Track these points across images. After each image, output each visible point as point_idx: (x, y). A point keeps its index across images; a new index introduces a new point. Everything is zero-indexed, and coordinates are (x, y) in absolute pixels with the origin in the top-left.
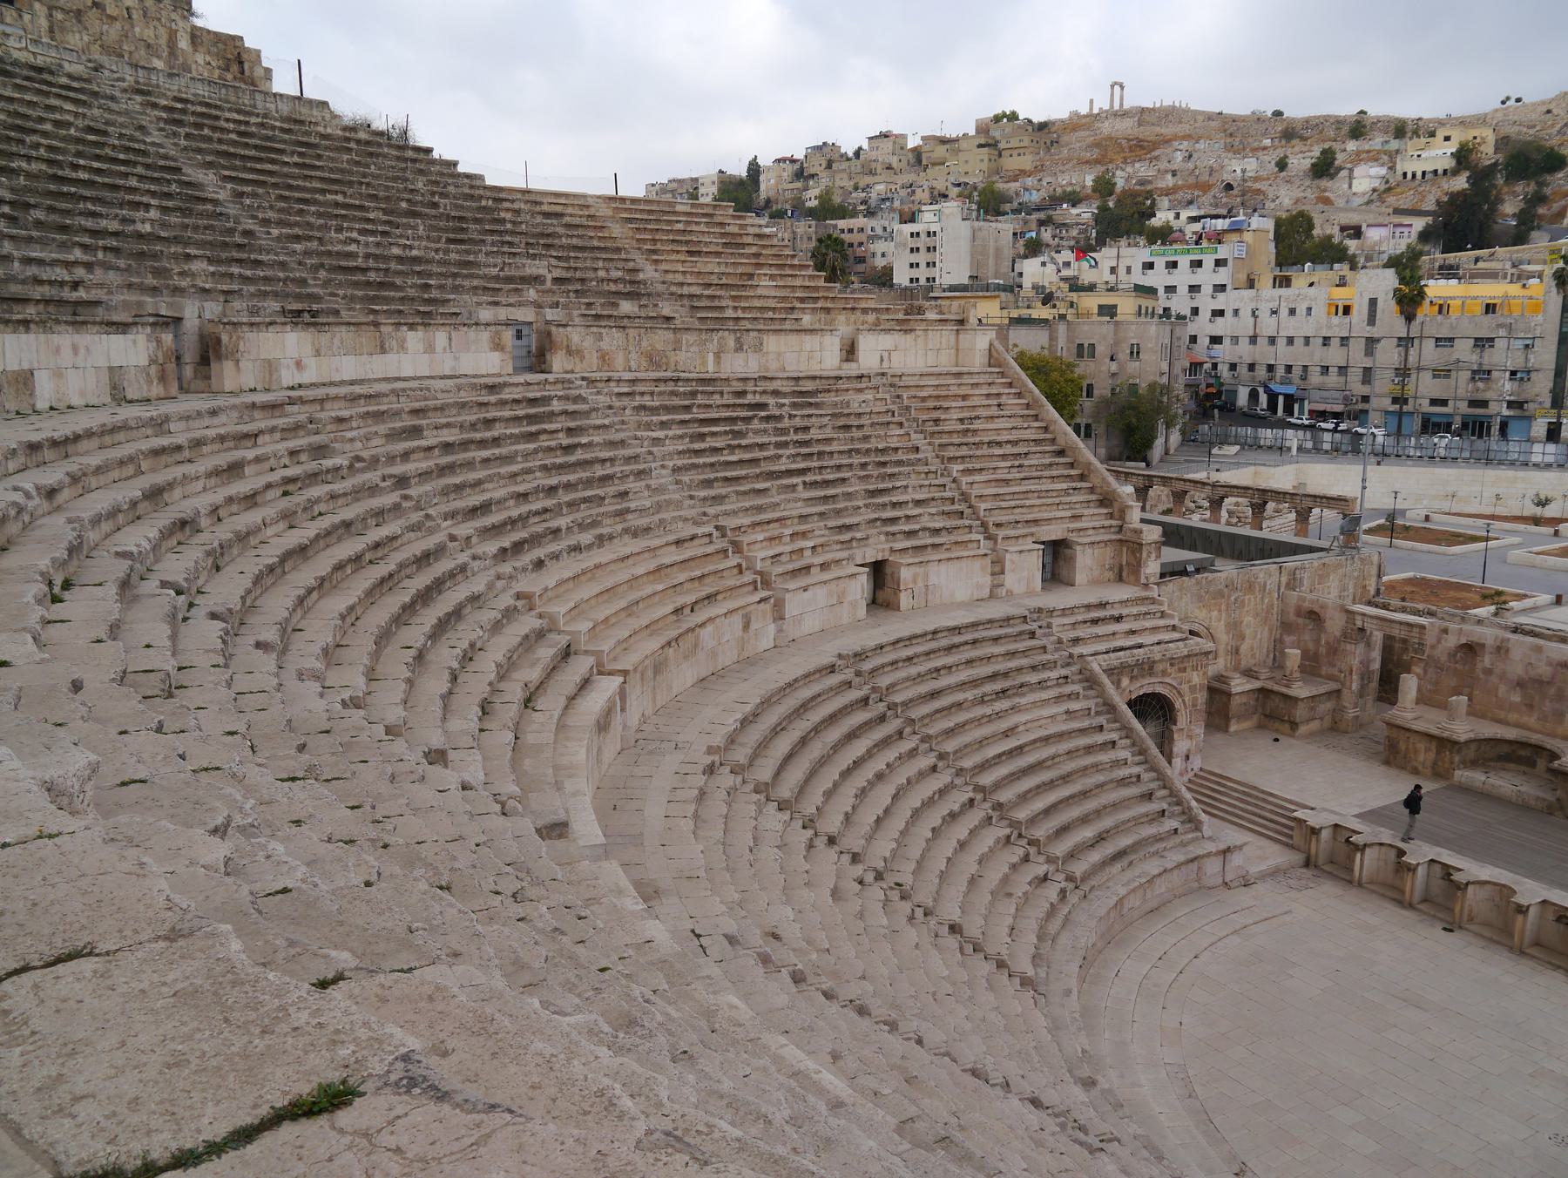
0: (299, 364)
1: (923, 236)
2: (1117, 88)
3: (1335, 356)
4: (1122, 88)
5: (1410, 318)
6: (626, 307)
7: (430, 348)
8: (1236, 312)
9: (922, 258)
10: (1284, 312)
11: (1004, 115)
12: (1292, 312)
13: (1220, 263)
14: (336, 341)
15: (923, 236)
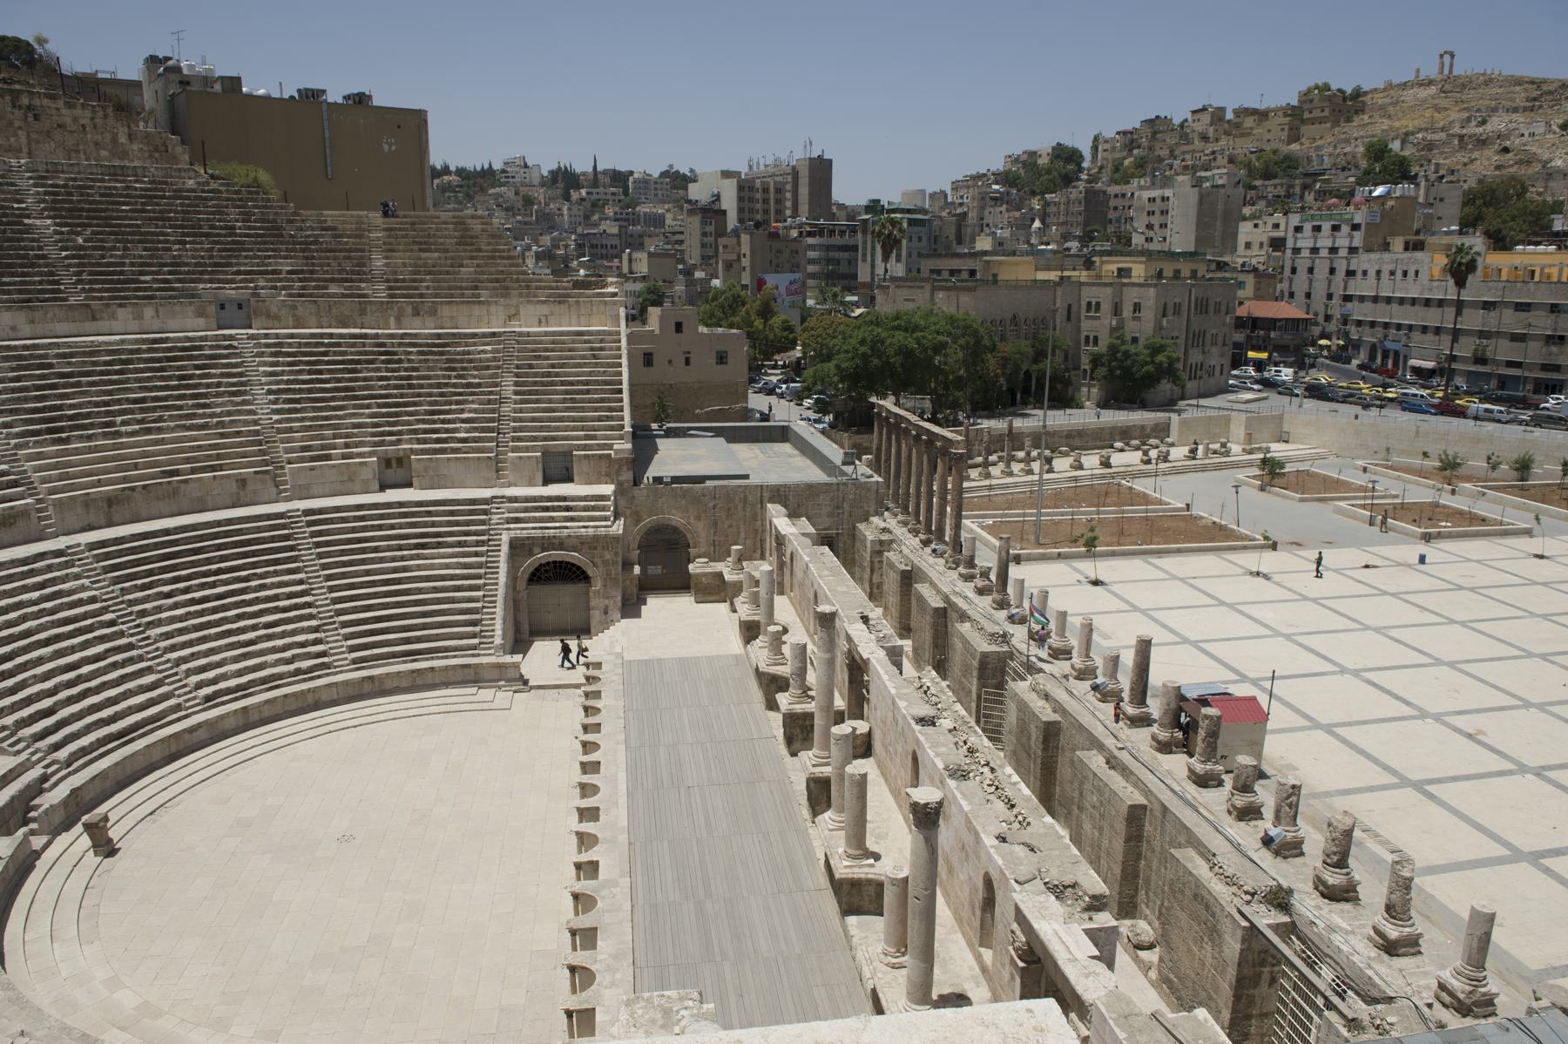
0: (13, 328)
1: (1158, 201)
2: (1447, 58)
3: (1432, 317)
4: (1452, 56)
5: (1460, 283)
6: (334, 289)
7: (140, 317)
8: (1365, 273)
9: (1156, 220)
10: (1399, 274)
11: (1317, 87)
12: (1405, 274)
13: (1355, 227)
14: (50, 315)
15: (1158, 201)
